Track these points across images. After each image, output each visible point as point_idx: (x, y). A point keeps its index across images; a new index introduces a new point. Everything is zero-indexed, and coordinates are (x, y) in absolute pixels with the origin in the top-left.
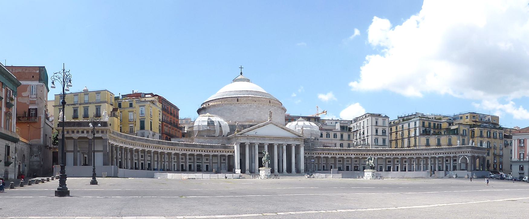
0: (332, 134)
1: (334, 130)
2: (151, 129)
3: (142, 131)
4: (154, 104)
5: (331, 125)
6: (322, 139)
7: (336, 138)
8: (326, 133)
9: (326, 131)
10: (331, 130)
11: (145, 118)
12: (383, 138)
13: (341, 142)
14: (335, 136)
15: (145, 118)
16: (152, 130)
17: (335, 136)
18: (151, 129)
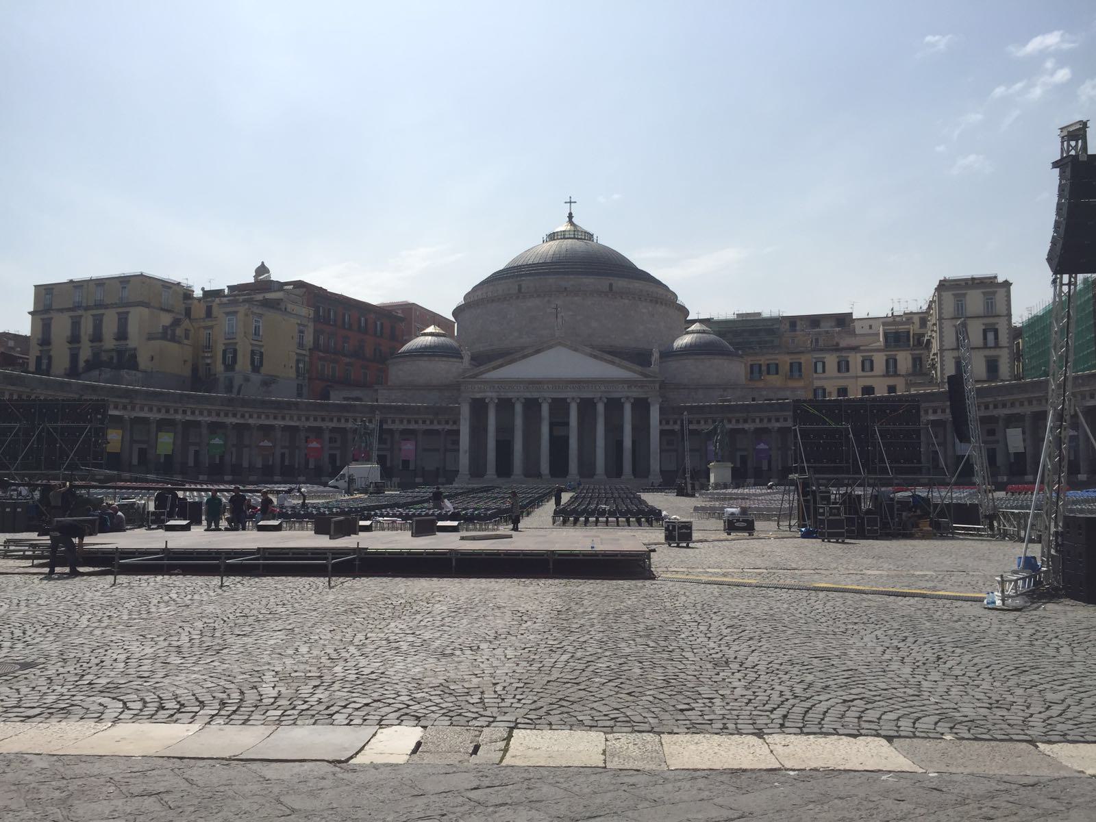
0: (855, 360)
1: (861, 348)
2: (256, 368)
3: (229, 374)
4: (280, 309)
5: (871, 331)
6: (826, 378)
7: (872, 369)
8: (837, 360)
9: (838, 354)
10: (855, 349)
11: (236, 343)
12: (985, 356)
13: (891, 381)
14: (868, 364)
15: (236, 343)
16: (263, 370)
17: (868, 364)
18: (256, 368)
